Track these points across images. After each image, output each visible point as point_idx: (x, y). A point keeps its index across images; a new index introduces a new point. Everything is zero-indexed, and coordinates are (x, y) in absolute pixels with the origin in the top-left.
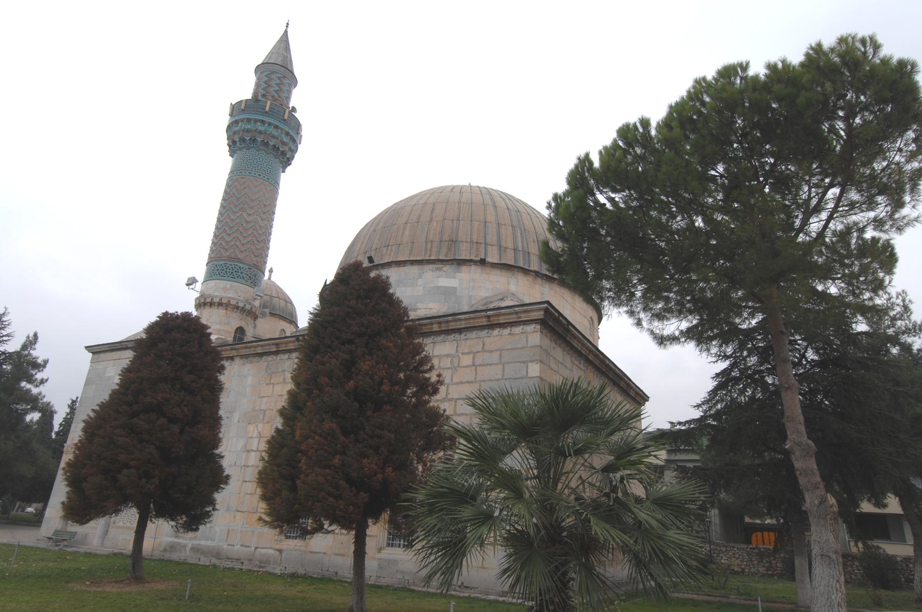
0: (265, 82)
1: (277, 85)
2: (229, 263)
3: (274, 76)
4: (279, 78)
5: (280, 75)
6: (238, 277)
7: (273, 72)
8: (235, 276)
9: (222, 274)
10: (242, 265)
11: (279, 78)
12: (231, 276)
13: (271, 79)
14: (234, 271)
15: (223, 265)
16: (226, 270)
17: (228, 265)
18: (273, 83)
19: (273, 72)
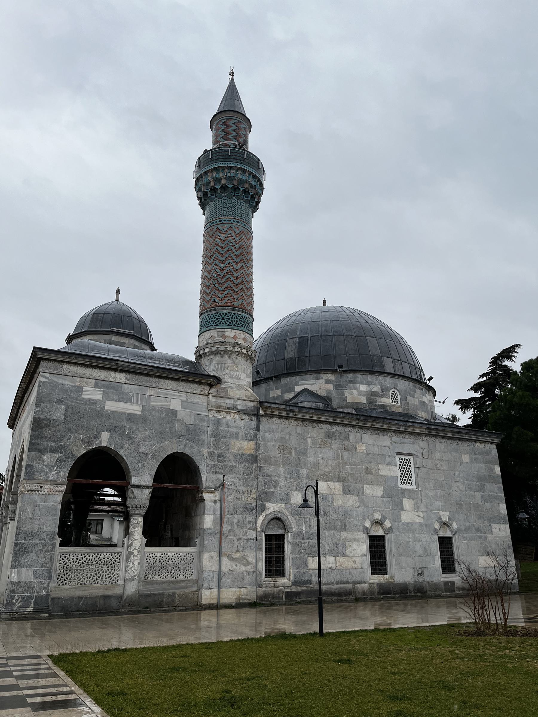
0: (222, 131)
1: (234, 130)
2: (233, 312)
3: (230, 123)
4: (234, 124)
5: (235, 121)
6: (242, 326)
7: (227, 120)
8: (240, 325)
9: (228, 323)
10: (242, 314)
11: (234, 124)
12: (237, 325)
13: (228, 126)
14: (238, 320)
15: (228, 315)
16: (231, 319)
17: (232, 314)
18: (230, 130)
19: (227, 120)
